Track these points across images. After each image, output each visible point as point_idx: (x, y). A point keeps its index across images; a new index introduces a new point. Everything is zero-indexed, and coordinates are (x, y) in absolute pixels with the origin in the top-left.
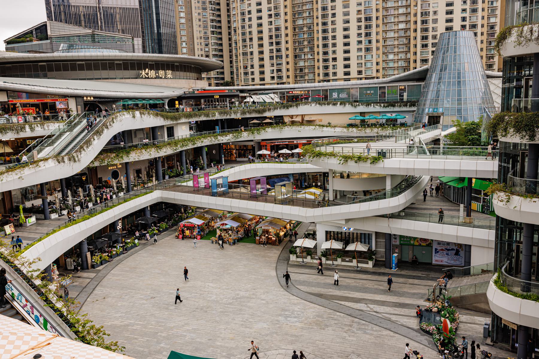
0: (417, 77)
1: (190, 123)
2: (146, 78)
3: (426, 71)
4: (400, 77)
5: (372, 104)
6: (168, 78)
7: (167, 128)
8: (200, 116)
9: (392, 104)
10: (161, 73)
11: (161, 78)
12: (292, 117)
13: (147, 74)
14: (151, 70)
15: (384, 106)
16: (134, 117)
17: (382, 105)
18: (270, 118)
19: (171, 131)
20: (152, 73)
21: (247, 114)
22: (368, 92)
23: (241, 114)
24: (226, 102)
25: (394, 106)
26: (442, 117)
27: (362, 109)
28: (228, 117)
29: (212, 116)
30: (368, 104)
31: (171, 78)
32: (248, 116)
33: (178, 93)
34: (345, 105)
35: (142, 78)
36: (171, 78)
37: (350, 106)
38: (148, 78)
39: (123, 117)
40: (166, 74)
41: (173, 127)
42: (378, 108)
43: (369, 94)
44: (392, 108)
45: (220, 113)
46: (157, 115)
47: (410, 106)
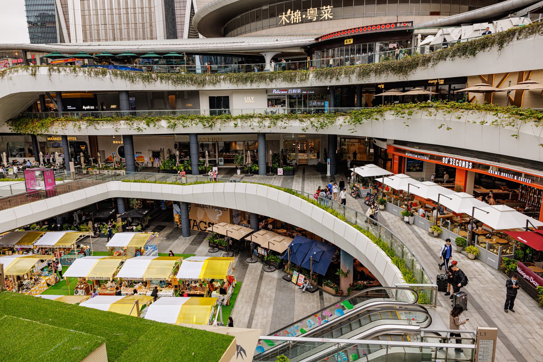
1: (267, 91)
2: (286, 24)
6: (324, 19)
7: (212, 99)
8: (271, 81)
10: (312, 12)
11: (311, 21)
12: (489, 79)
13: (289, 18)
14: (295, 11)
16: (34, 74)
18: (424, 84)
19: (220, 103)
20: (297, 15)
21: (373, 75)
23: (359, 75)
24: (371, 50)
28: (334, 83)
29: (301, 80)
31: (329, 19)
32: (373, 79)
33: (309, 40)
35: (281, 25)
36: (329, 19)
38: (290, 24)
39: (16, 74)
40: (320, 13)
41: (228, 97)
45: (319, 75)
46: (104, 73)
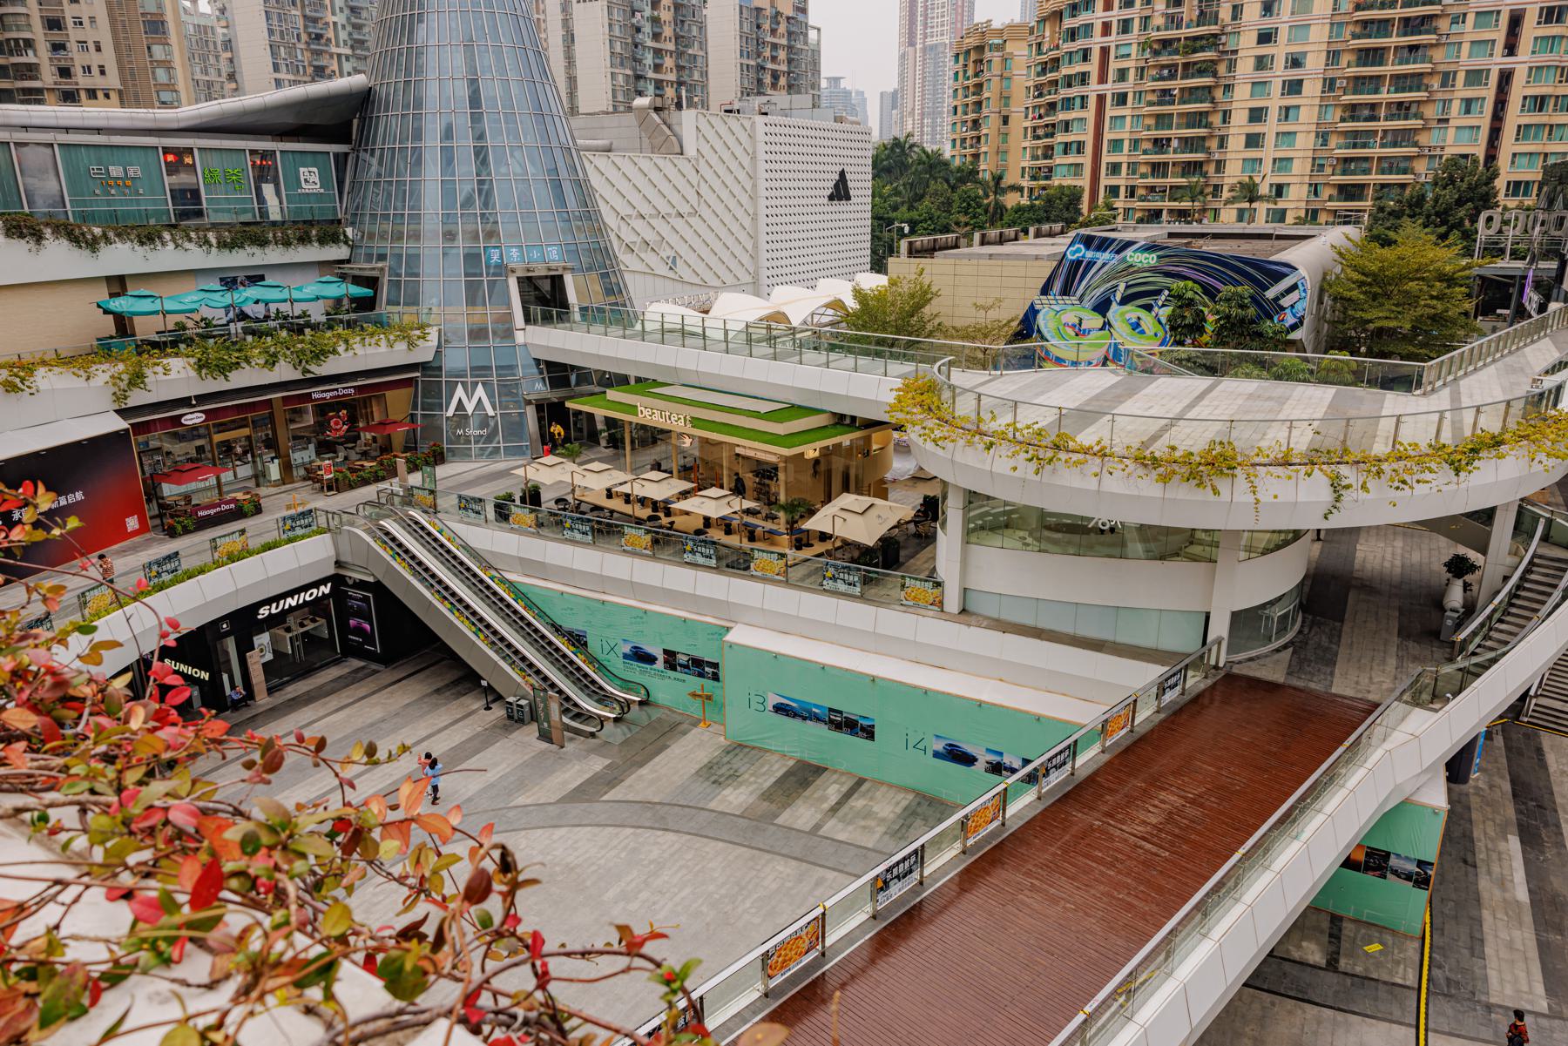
0: (289, 120)
3: (363, 101)
4: (224, 115)
5: (167, 236)
9: (252, 233)
15: (222, 245)
17: (212, 237)
22: (116, 171)
25: (262, 243)
26: (569, 280)
27: (122, 257)
30: (148, 237)
34: (39, 238)
37: (64, 242)
42: (194, 257)
43: (125, 183)
44: (256, 250)
47: (322, 241)
